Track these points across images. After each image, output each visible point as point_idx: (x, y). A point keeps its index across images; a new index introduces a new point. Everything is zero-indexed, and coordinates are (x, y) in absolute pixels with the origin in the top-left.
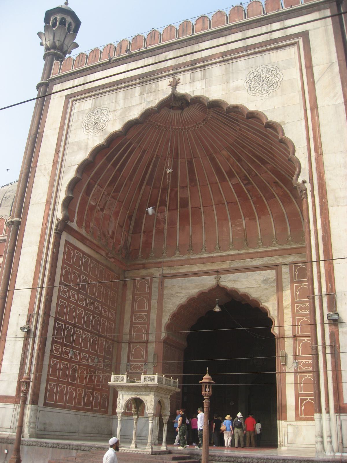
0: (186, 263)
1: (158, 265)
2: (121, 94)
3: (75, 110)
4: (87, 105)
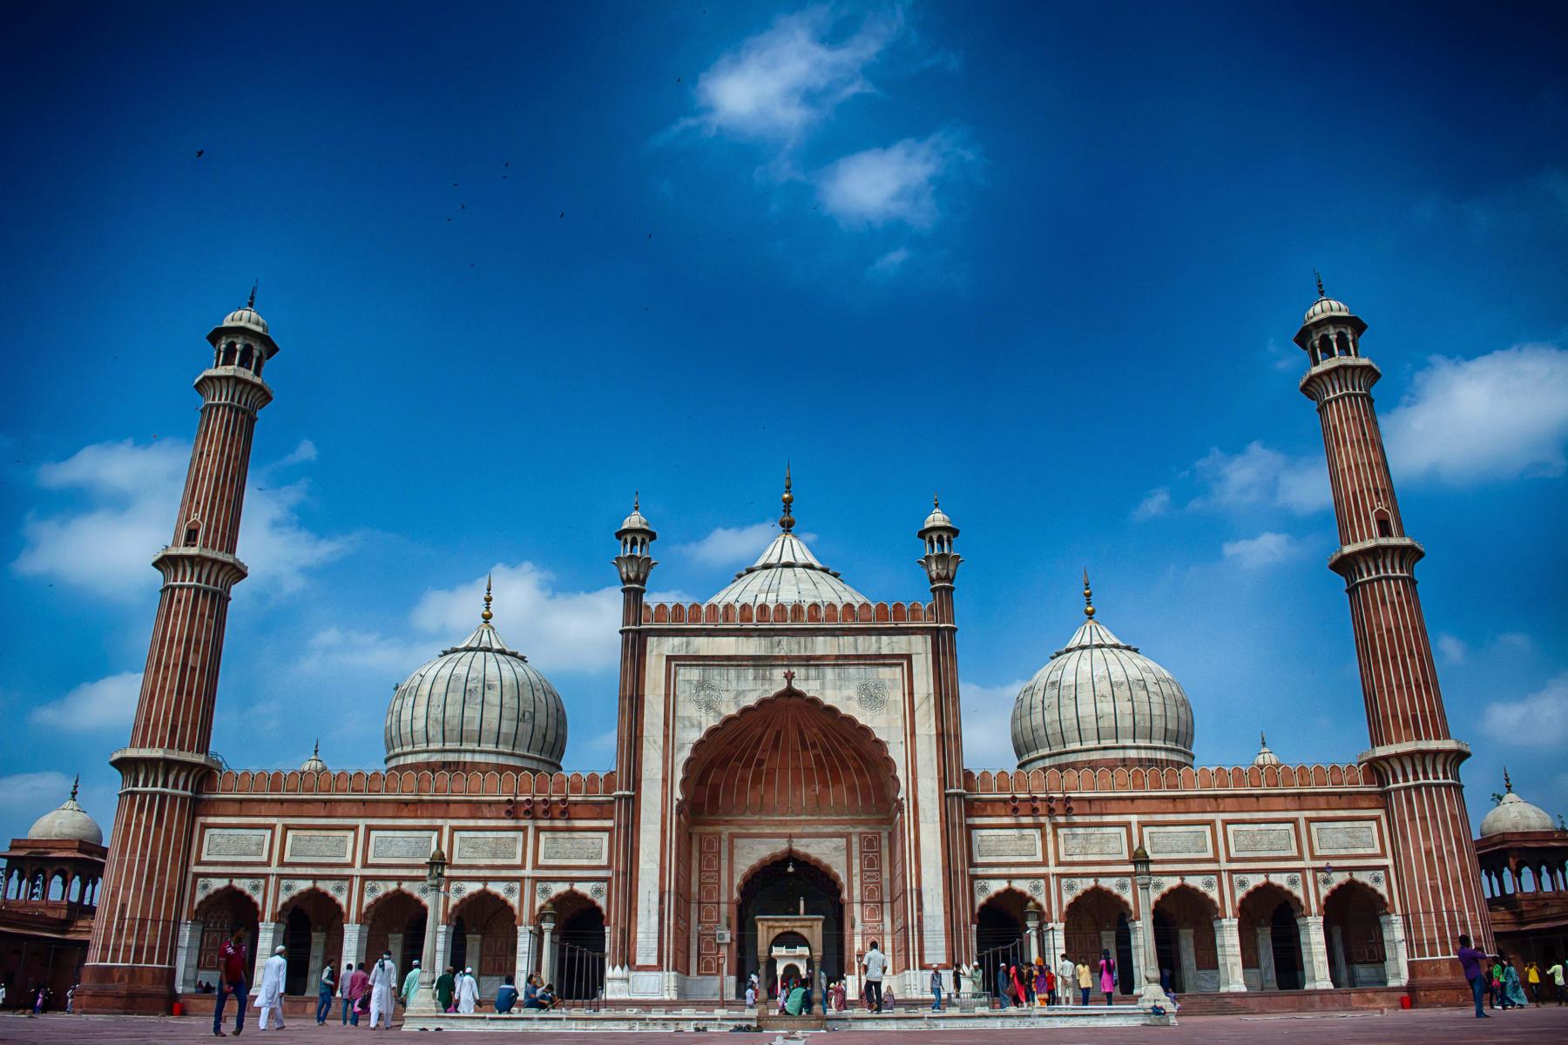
0: (756, 823)
1: (728, 823)
2: (732, 672)
3: (680, 678)
4: (694, 674)
